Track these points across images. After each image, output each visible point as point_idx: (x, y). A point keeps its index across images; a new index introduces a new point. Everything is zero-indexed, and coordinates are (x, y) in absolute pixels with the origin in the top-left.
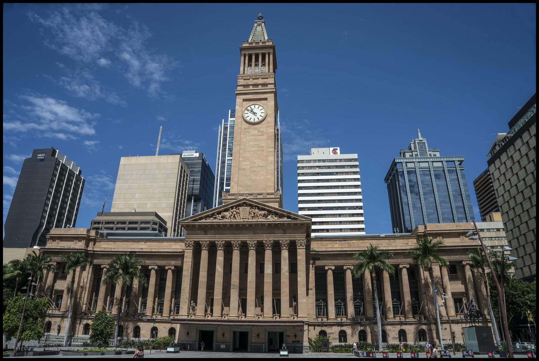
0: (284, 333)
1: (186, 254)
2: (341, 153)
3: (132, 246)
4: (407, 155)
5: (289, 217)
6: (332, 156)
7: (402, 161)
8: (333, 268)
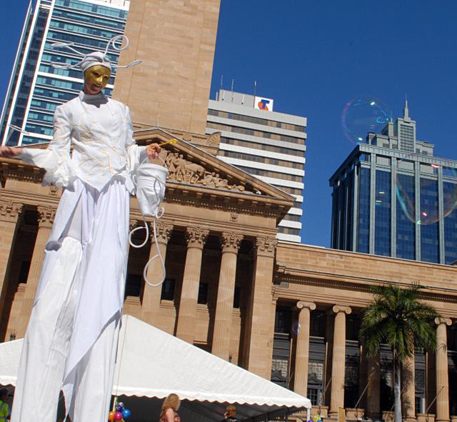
2: (274, 110)
4: (380, 142)
5: (249, 187)
6: (256, 111)
7: (370, 150)
8: (313, 307)
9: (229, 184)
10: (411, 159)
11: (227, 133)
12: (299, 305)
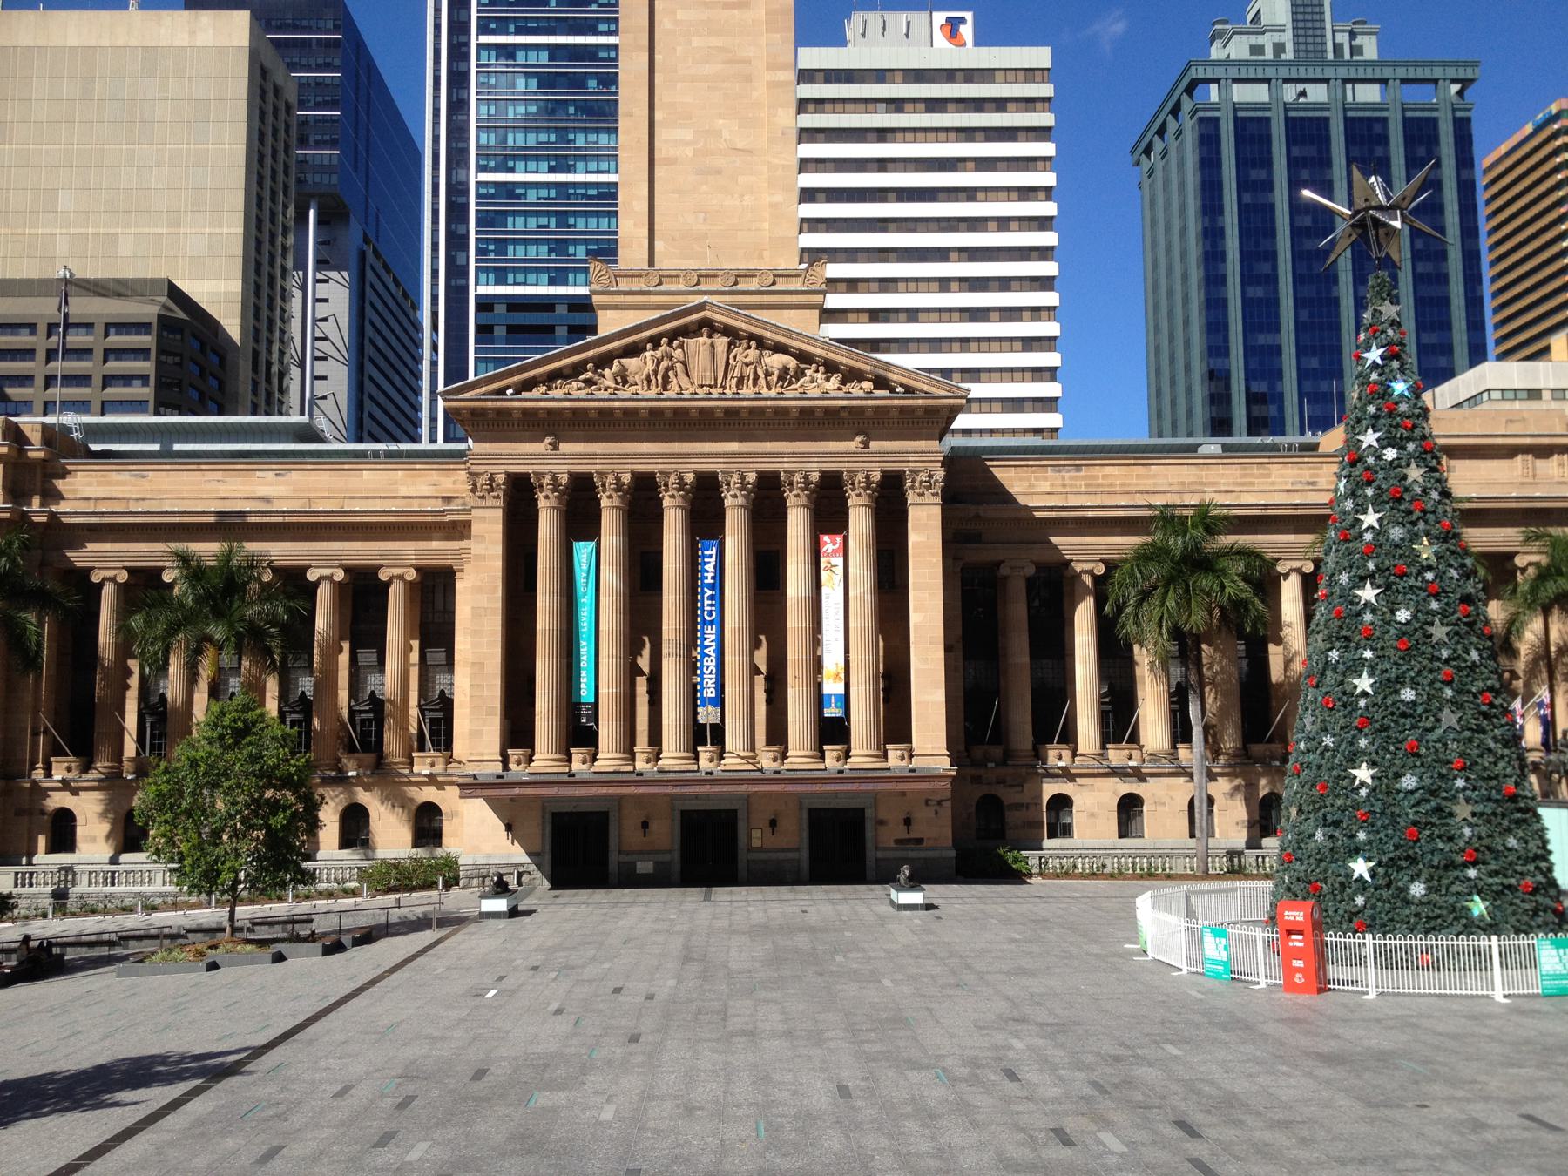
0: (869, 813)
1: (474, 527)
2: (977, 43)
3: (224, 490)
5: (881, 382)
6: (942, 54)
8: (1031, 570)
9: (843, 382)
10: (1319, 75)
11: (835, 270)
12: (1004, 571)
